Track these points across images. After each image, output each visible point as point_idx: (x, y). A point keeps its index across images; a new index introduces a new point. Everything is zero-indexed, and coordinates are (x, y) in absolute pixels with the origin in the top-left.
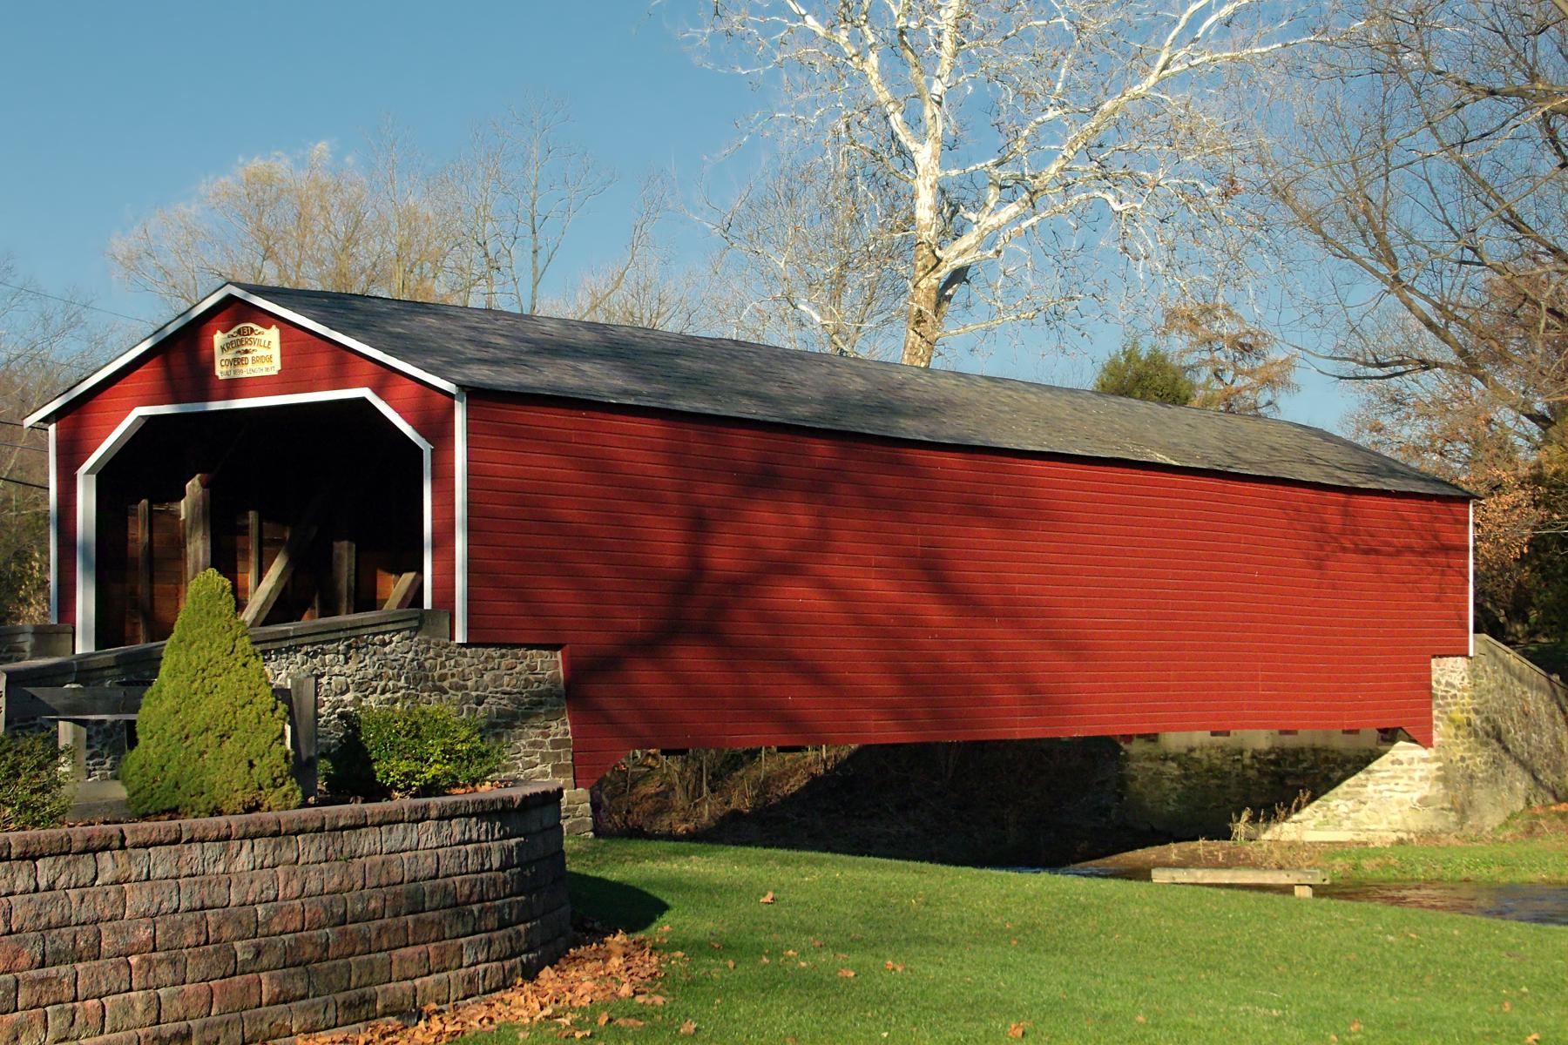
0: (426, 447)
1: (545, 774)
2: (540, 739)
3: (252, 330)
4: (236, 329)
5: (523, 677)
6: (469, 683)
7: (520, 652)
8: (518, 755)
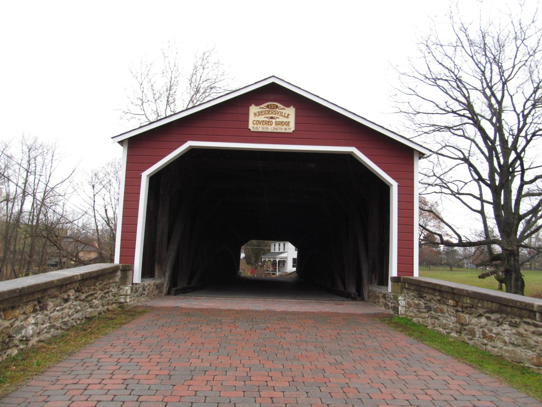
3: (277, 107)
4: (266, 104)
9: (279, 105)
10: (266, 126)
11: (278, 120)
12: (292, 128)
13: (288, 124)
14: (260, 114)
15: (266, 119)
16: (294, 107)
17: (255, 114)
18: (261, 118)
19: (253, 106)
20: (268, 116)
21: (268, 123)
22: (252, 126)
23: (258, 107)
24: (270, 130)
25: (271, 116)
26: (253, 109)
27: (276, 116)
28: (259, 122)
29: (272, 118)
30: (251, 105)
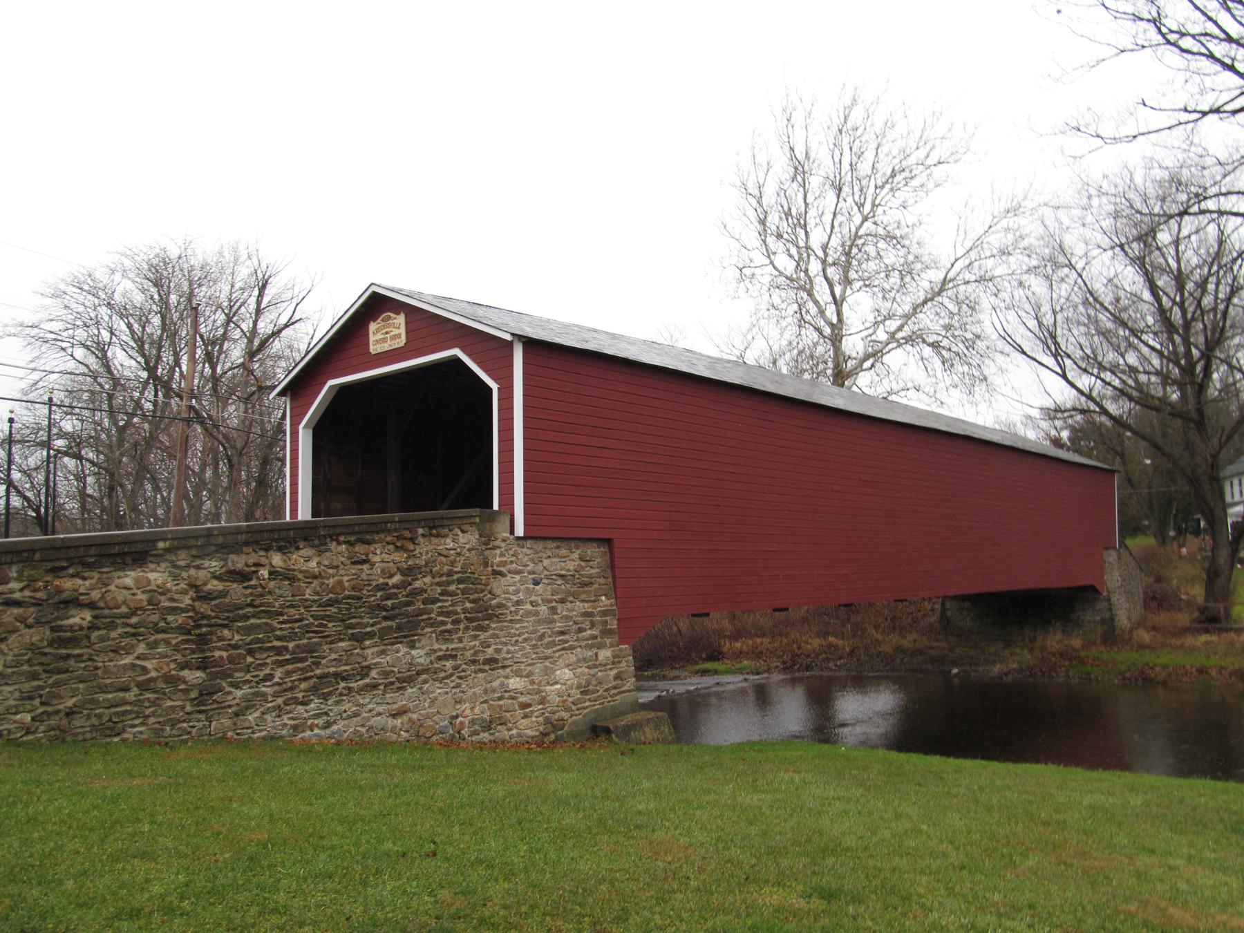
0: (494, 386)
3: (390, 317)
9: (391, 314)
11: (392, 334)
12: (402, 341)
13: (399, 336)
14: (377, 331)
15: (383, 336)
18: (379, 336)
21: (384, 340)
22: (374, 349)
24: (386, 349)
26: (373, 327)
28: (377, 342)
29: (387, 333)
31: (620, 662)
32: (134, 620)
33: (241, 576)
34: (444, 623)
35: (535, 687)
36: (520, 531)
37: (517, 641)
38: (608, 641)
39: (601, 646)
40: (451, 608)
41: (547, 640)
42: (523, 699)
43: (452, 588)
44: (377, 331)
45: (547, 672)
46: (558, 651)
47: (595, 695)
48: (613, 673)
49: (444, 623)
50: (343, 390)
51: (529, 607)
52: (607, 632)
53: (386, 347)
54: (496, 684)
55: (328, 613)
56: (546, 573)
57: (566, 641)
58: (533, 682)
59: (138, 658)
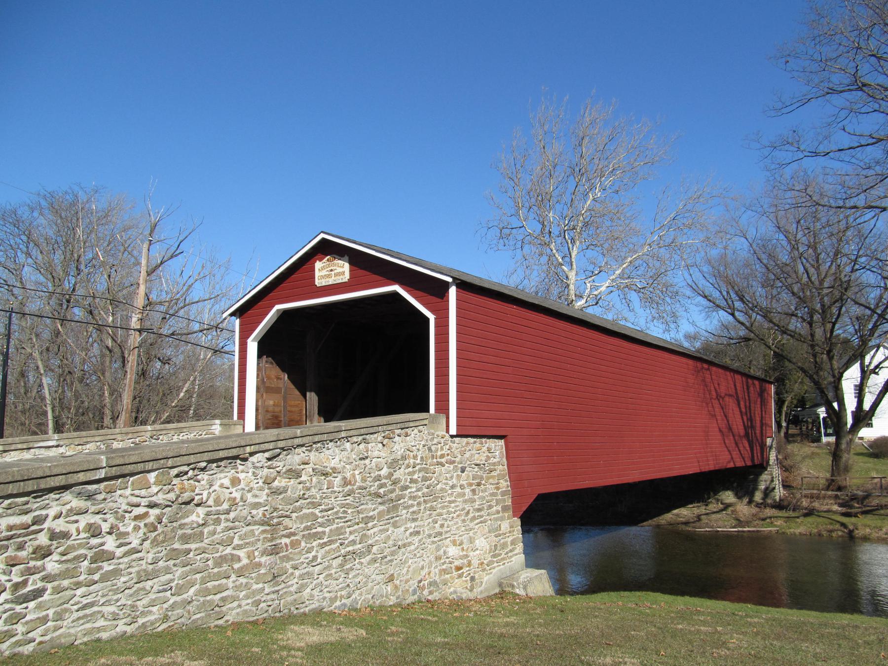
0: (432, 317)
1: (498, 512)
2: (495, 491)
5: (485, 455)
6: (457, 460)
7: (484, 440)
8: (484, 502)
10: (327, 279)
11: (336, 271)
12: (346, 277)
14: (323, 268)
15: (328, 273)
16: (348, 255)
17: (319, 270)
18: (324, 273)
19: (318, 261)
20: (328, 269)
21: (329, 276)
22: (318, 282)
23: (321, 263)
24: (330, 283)
25: (330, 269)
26: (318, 265)
27: (334, 268)
28: (322, 277)
29: (331, 270)
30: (316, 262)
31: (514, 531)
32: (232, 515)
33: (294, 474)
34: (412, 506)
35: (465, 553)
36: (453, 430)
37: (453, 518)
38: (506, 515)
39: (502, 519)
40: (416, 494)
41: (471, 515)
42: (457, 563)
43: (416, 477)
44: (323, 268)
45: (471, 540)
46: (477, 524)
47: (499, 558)
48: (509, 539)
49: (412, 506)
50: (285, 313)
51: (458, 490)
52: (505, 509)
53: (331, 281)
54: (441, 552)
55: (347, 501)
56: (469, 463)
57: (481, 516)
58: (463, 549)
59: (234, 549)
